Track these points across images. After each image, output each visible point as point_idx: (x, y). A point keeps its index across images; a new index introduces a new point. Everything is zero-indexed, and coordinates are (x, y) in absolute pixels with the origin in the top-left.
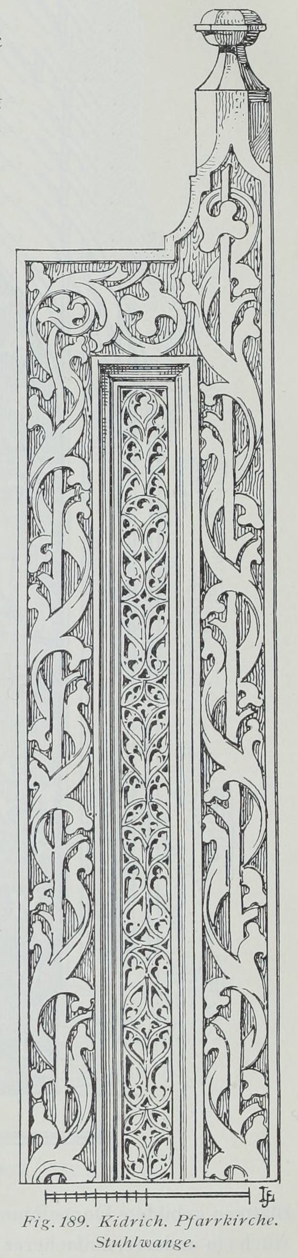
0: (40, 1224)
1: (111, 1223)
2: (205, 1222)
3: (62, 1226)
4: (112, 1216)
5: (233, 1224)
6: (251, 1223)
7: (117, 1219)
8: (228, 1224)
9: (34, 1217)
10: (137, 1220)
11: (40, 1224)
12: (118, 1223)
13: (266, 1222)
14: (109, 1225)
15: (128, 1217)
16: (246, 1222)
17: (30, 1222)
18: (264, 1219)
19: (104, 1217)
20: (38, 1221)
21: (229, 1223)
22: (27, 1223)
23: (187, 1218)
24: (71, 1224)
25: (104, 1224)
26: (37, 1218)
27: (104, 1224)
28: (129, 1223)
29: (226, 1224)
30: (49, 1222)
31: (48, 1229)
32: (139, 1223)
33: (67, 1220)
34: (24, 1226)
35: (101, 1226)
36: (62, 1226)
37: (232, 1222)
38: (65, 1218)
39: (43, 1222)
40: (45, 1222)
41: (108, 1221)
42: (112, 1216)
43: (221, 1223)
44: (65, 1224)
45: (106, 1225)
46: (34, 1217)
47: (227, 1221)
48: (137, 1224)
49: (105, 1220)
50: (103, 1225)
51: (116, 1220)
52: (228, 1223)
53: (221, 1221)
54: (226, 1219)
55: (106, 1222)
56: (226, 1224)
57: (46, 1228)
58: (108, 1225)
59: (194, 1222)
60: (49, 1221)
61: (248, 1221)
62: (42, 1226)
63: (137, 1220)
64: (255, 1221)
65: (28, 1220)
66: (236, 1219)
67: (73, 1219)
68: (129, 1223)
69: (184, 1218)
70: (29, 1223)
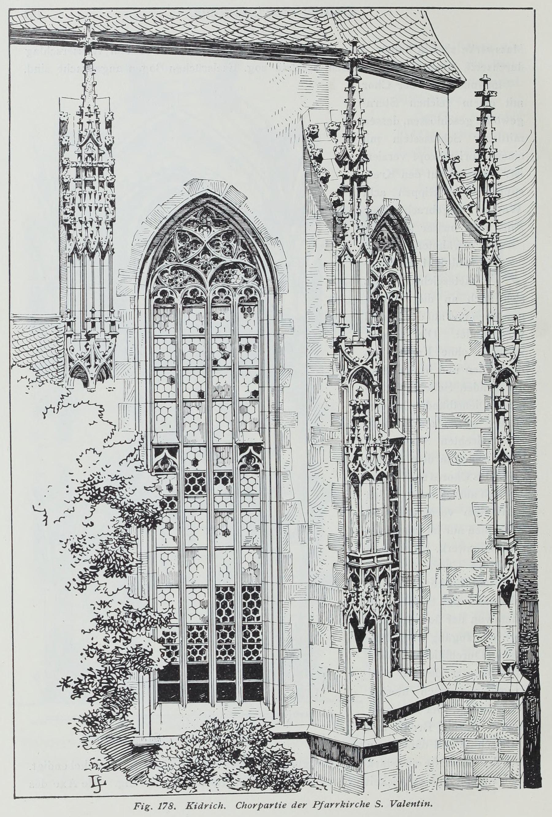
1: (193, 806)
2: (330, 805)
4: (193, 803)
9: (140, 803)
11: (144, 807)
12: (197, 807)
25: (189, 807)
27: (189, 807)
32: (209, 807)
34: (135, 809)
36: (159, 808)
37: (346, 805)
42: (193, 803)
46: (140, 803)
58: (191, 808)
59: (323, 805)
68: (204, 807)
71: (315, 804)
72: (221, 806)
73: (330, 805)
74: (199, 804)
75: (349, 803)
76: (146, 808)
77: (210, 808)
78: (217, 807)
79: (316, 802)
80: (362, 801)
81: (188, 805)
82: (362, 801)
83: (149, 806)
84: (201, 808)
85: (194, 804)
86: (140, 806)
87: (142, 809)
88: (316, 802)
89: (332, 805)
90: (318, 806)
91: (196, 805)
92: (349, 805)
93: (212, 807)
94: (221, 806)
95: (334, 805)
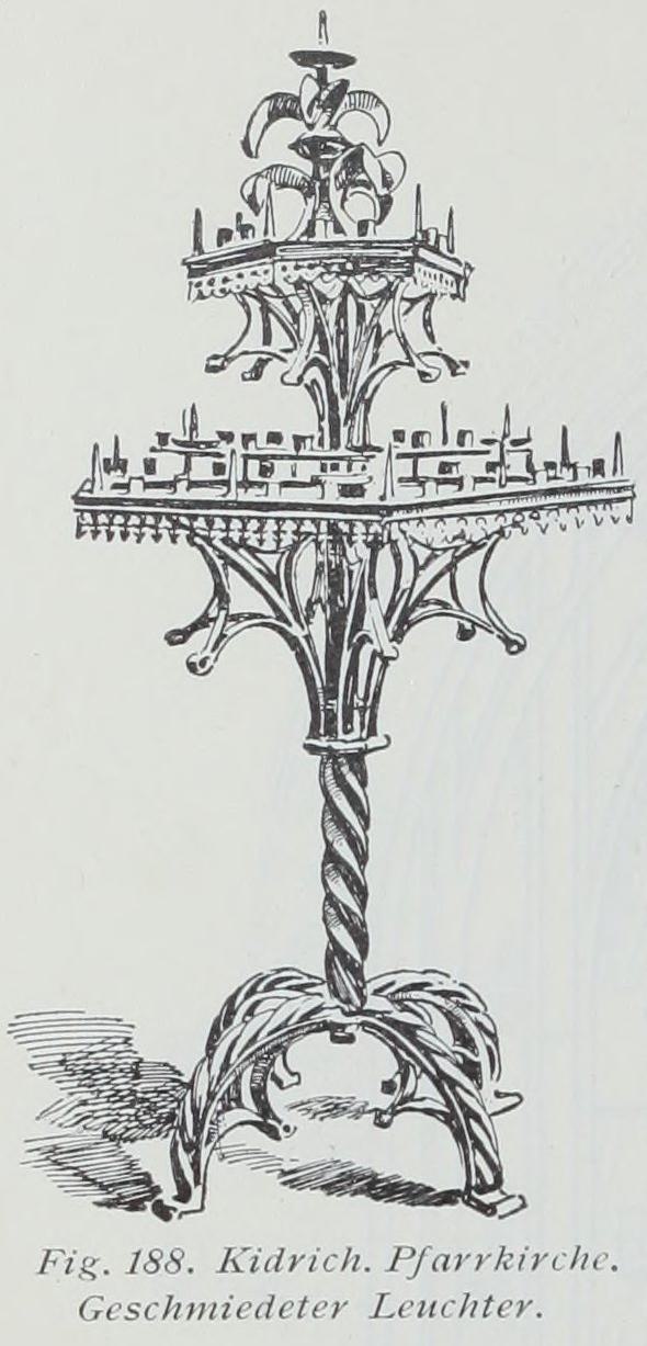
1: (245, 1264)
3: (132, 1271)
4: (245, 1249)
7: (259, 1254)
8: (506, 1268)
9: (63, 1251)
10: (303, 1257)
12: (260, 1264)
13: (590, 1262)
14: (241, 1268)
15: (283, 1250)
16: (546, 1264)
17: (54, 1262)
19: (230, 1251)
20: (71, 1260)
21: (508, 1264)
22: (49, 1264)
23: (414, 1252)
24: (152, 1267)
25: (230, 1266)
26: (68, 1256)
27: (230, 1266)
28: (286, 1262)
29: (501, 1266)
30: (97, 1264)
31: (94, 1276)
32: (306, 1263)
33: (144, 1258)
34: (42, 1271)
35: (223, 1270)
36: (132, 1271)
37: (517, 1259)
38: (138, 1254)
40: (89, 1262)
41: (237, 1261)
42: (245, 1249)
43: (490, 1263)
45: (234, 1269)
46: (63, 1251)
47: (504, 1259)
48: (303, 1265)
49: (231, 1257)
50: (227, 1268)
51: (256, 1258)
53: (546, 1259)
54: (502, 1255)
55: (234, 1261)
56: (501, 1266)
58: (237, 1270)
60: (98, 1260)
62: (80, 1271)
63: (303, 1257)
65: (51, 1258)
66: (523, 1256)
67: (156, 1255)
68: (286, 1262)
69: (405, 1253)
70: (52, 1264)
84: (276, 1268)
92: (530, 1261)
93: (319, 1264)
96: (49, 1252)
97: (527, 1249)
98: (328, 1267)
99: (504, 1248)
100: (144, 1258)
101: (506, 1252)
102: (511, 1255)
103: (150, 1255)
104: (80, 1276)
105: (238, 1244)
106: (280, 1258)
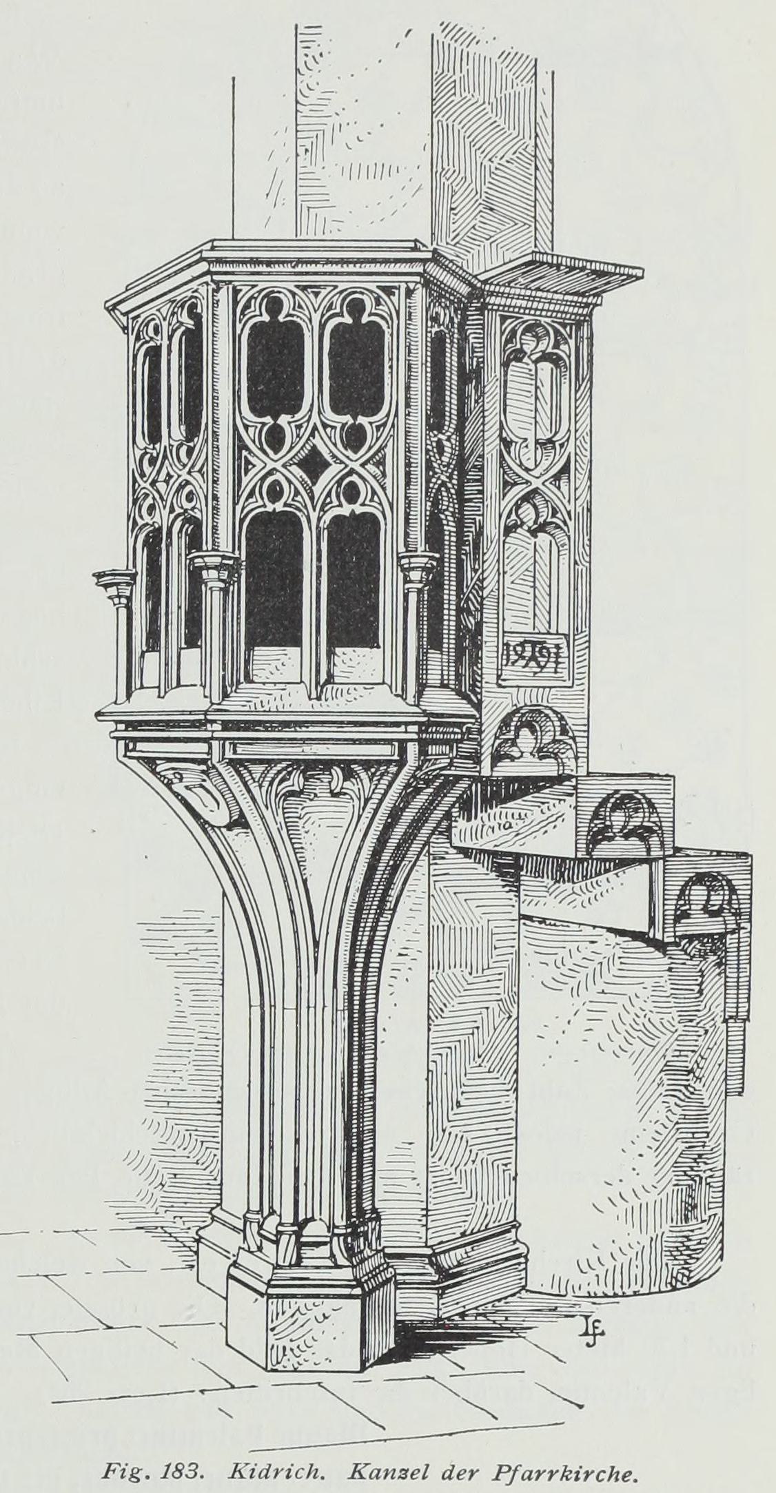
0: (128, 1474)
1: (246, 1473)
2: (534, 1475)
4: (247, 1464)
5: (573, 1479)
6: (600, 1478)
8: (567, 1479)
9: (119, 1464)
10: (282, 1469)
11: (128, 1474)
12: (256, 1474)
13: (620, 1477)
15: (270, 1465)
16: (592, 1477)
17: (114, 1471)
18: (618, 1473)
20: (124, 1470)
21: (569, 1477)
22: (111, 1473)
23: (510, 1468)
24: (177, 1474)
25: (237, 1475)
26: (122, 1467)
27: (237, 1475)
29: (564, 1478)
30: (140, 1472)
31: (139, 1480)
32: (284, 1474)
33: (172, 1468)
34: (106, 1477)
35: (353, 1477)
36: (165, 1477)
37: (573, 1475)
38: (168, 1466)
39: (132, 1470)
40: (135, 1471)
42: (247, 1464)
43: (557, 1476)
44: (169, 1474)
46: (119, 1464)
47: (566, 1474)
48: (283, 1474)
49: (238, 1469)
50: (235, 1476)
52: (567, 1477)
54: (565, 1471)
56: (564, 1478)
57: (136, 1480)
58: (242, 1477)
59: (518, 1475)
61: (594, 1476)
64: (605, 1476)
65: (112, 1468)
66: (578, 1473)
67: (180, 1467)
68: (271, 1473)
69: (505, 1469)
71: (500, 1472)
72: (313, 1472)
73: (534, 1475)
74: (262, 1466)
75: (582, 1471)
76: (132, 1476)
77: (288, 1477)
78: (303, 1474)
79: (501, 1467)
80: (613, 1468)
81: (235, 1471)
82: (613, 1468)
83: (139, 1470)
84: (266, 1477)
85: (249, 1467)
86: (119, 1469)
87: (122, 1477)
88: (501, 1467)
89: (539, 1474)
90: (505, 1478)
91: (253, 1470)
92: (582, 1476)
93: (293, 1473)
94: (313, 1472)
95: (546, 1475)
96: (110, 1465)
97: (581, 1467)
98: (299, 1476)
99: (566, 1466)
100: (172, 1468)
101: (568, 1469)
102: (571, 1472)
103: (176, 1467)
104: (130, 1480)
105: (242, 1461)
106: (268, 1470)
